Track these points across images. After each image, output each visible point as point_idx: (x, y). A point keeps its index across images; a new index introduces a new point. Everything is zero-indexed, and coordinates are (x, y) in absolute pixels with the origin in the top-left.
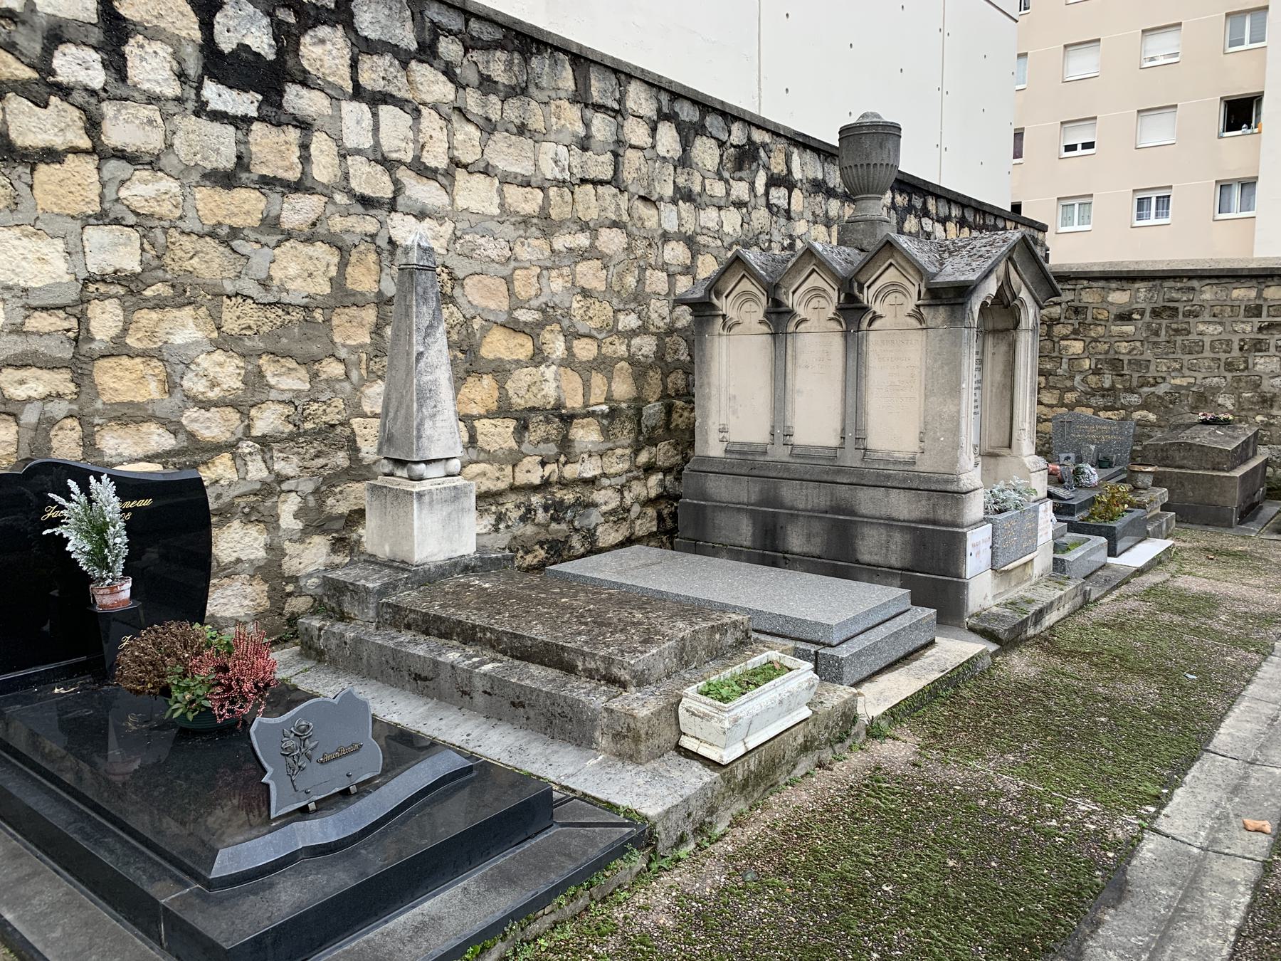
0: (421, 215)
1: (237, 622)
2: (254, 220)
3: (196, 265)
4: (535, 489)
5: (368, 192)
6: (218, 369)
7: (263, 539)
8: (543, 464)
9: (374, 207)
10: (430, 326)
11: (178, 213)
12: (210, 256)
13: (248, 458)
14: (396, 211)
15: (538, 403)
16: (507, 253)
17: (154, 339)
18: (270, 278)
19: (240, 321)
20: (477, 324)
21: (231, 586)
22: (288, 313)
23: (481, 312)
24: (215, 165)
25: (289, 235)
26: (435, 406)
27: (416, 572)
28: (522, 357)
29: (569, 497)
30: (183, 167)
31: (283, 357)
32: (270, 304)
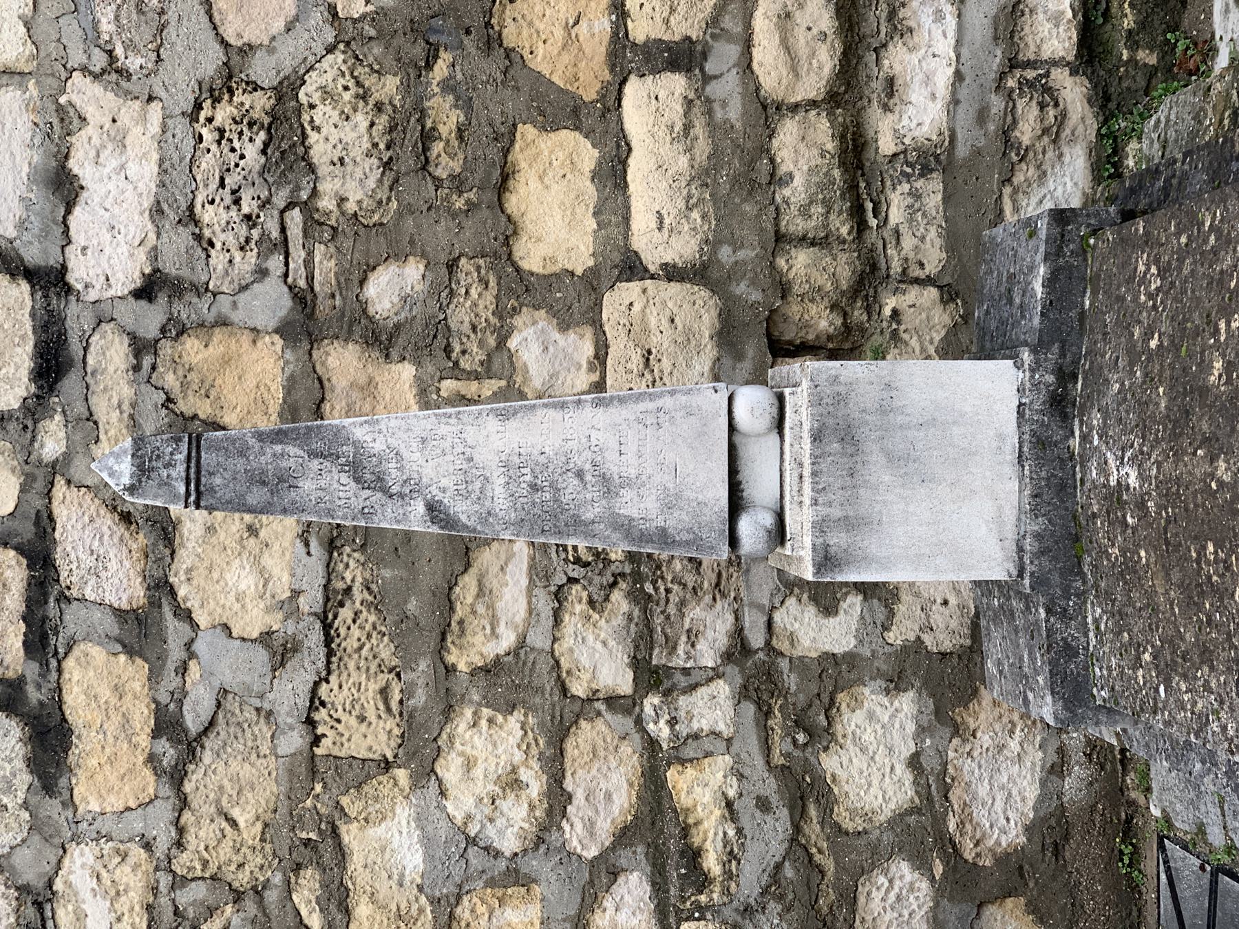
1: (1057, 769)
2: (134, 673)
3: (250, 816)
5: (22, 358)
6: (478, 772)
7: (872, 695)
10: (355, 469)
11: (137, 853)
12: (226, 782)
14: (64, 268)
17: (414, 912)
18: (266, 637)
19: (371, 715)
21: (968, 784)
22: (348, 590)
24: (19, 764)
25: (161, 588)
26: (580, 474)
27: (1039, 583)
30: (36, 838)
31: (452, 609)
32: (328, 641)
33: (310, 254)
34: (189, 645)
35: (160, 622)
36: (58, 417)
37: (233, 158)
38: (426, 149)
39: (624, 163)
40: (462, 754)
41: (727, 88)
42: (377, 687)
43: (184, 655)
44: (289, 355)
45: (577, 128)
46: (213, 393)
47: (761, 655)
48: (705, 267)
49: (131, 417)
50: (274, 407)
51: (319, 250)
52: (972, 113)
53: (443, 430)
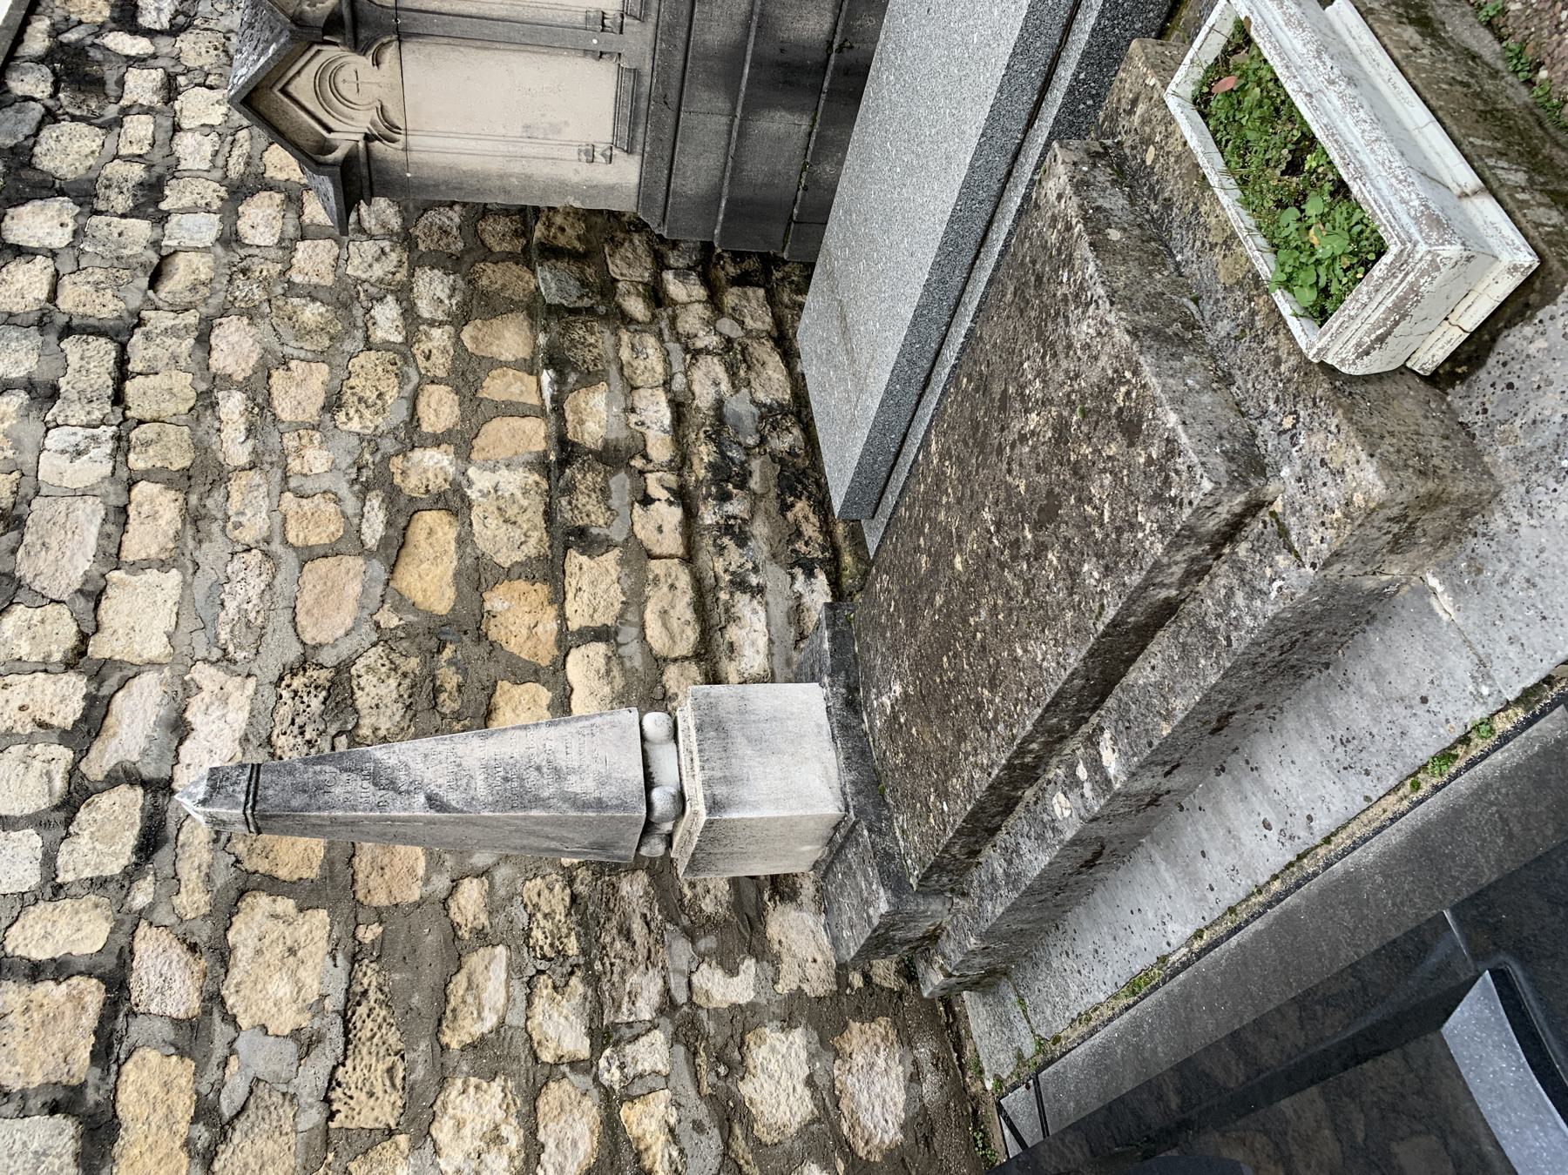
0: (179, 728)
1: (915, 1078)
2: (181, 1070)
4: (690, 516)
5: (131, 838)
6: (467, 1131)
8: (647, 501)
9: (162, 825)
10: (374, 778)
12: (251, 1160)
13: (630, 1071)
14: (171, 779)
15: (536, 506)
16: (255, 557)
18: (296, 1033)
19: (379, 1090)
20: (390, 620)
21: (853, 1095)
22: (365, 993)
23: (367, 612)
24: (68, 1159)
25: (214, 999)
26: (539, 769)
27: (860, 812)
28: (452, 534)
29: (705, 453)
31: (447, 1001)
32: (346, 1032)
34: (231, 1044)
35: (209, 1027)
36: (150, 878)
37: (302, 707)
38: (435, 698)
39: (569, 698)
40: (453, 1117)
41: (632, 650)
42: (385, 1067)
43: (226, 1052)
45: (537, 681)
46: (271, 856)
47: (685, 1008)
49: (207, 875)
50: (316, 863)
52: (782, 660)
53: (441, 748)
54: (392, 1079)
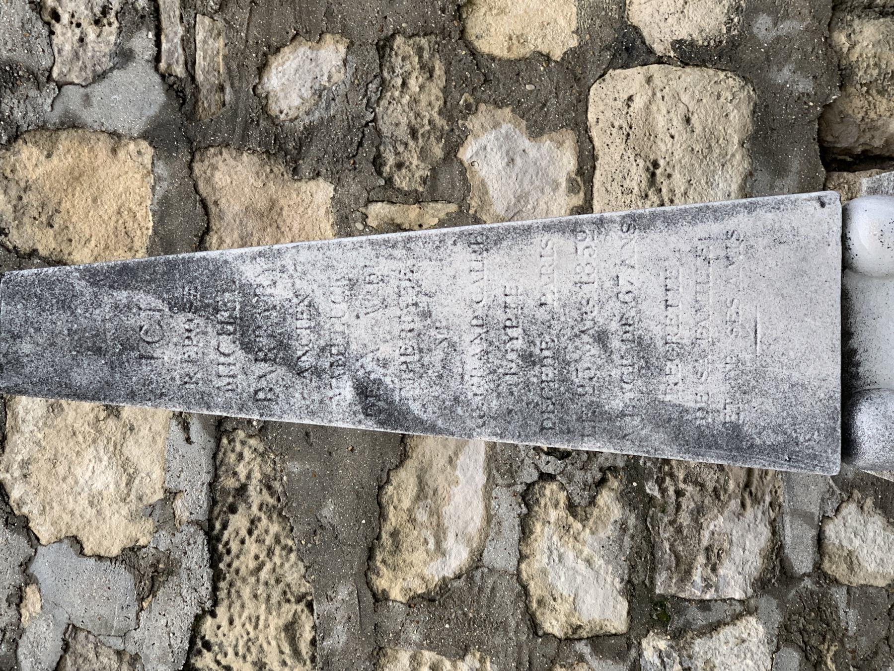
22: (242, 490)
31: (382, 516)
32: (214, 559)
33: (190, 30)
42: (281, 622)
43: (18, 579)
44: (161, 169)
46: (58, 221)
47: (808, 583)
48: (734, 44)
50: (141, 242)
51: (203, 25)
53: (384, 267)
54: (293, 642)
